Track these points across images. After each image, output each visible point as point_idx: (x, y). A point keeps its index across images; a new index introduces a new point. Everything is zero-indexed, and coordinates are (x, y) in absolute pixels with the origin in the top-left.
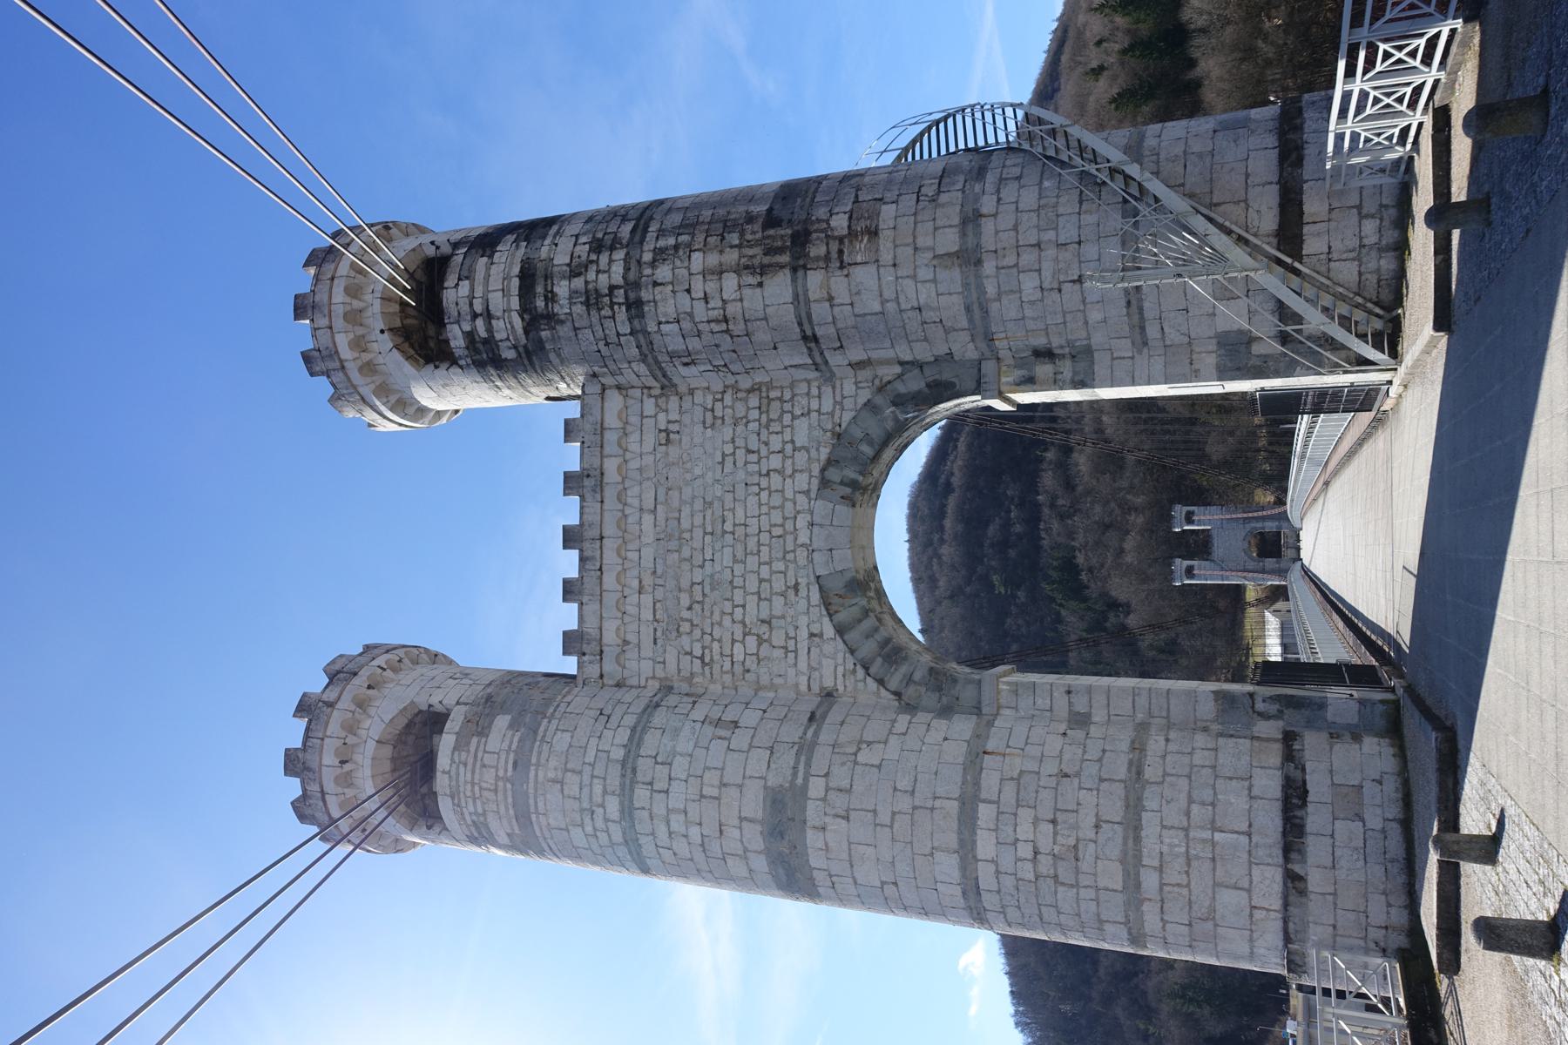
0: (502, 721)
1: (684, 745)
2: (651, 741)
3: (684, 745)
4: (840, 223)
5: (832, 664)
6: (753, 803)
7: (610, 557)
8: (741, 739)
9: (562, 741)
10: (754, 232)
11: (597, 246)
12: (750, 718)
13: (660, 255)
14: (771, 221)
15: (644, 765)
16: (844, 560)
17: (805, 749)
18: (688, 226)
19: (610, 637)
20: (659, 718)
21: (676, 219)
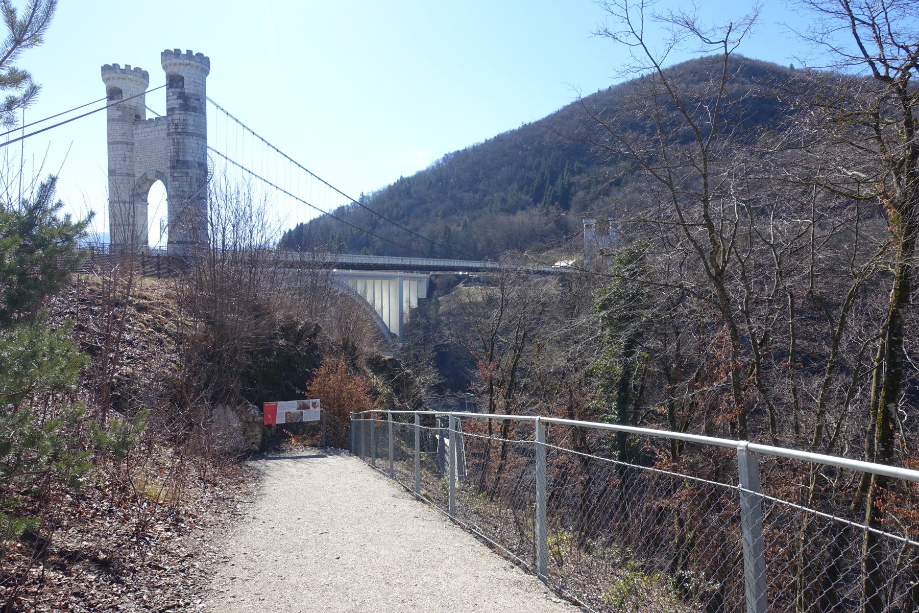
0: (120, 113)
1: (120, 152)
2: (120, 146)
3: (120, 152)
4: (176, 174)
5: (138, 176)
6: (113, 167)
7: (148, 129)
8: (122, 163)
9: (118, 128)
10: (176, 158)
11: (176, 125)
12: (127, 163)
13: (173, 139)
14: (177, 161)
15: (115, 146)
16: (149, 177)
17: (121, 175)
18: (178, 143)
19: (139, 131)
20: (125, 146)
21: (181, 141)
